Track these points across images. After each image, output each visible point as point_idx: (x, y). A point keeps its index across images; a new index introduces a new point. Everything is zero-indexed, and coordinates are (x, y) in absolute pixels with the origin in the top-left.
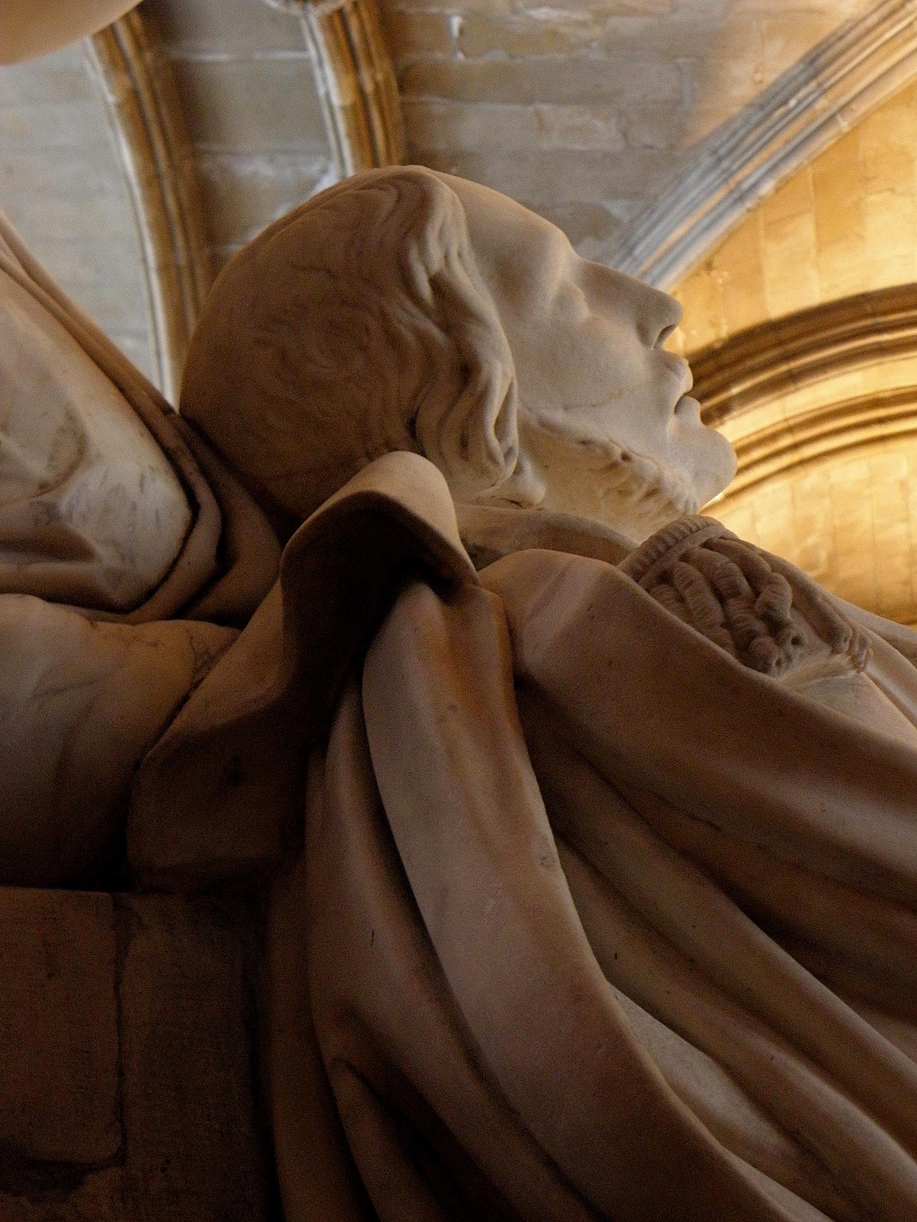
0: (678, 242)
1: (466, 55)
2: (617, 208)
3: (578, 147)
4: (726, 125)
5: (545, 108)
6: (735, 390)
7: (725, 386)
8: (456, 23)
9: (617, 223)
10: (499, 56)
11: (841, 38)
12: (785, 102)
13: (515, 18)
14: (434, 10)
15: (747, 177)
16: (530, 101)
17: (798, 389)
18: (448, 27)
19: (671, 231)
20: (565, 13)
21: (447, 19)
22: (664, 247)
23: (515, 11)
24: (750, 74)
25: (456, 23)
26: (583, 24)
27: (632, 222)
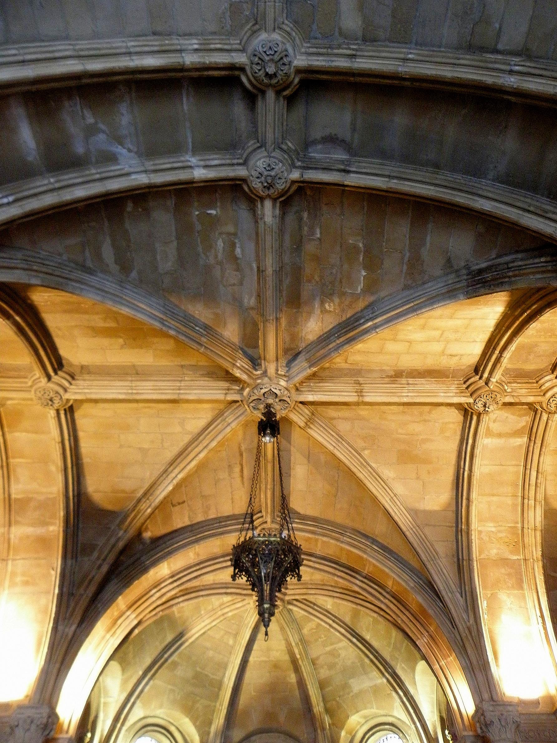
0: (138, 306)
1: (197, 215)
2: (134, 274)
3: (158, 257)
4: (176, 305)
5: (175, 243)
6: (18, 318)
7: (18, 314)
8: (213, 212)
9: (127, 276)
10: (198, 227)
11: (221, 337)
12: (196, 326)
13: (217, 234)
14: (218, 204)
15: (169, 322)
16: (178, 238)
17: (18, 336)
18: (211, 209)
19: (142, 303)
20: (221, 251)
21: (214, 208)
22: (136, 302)
23: (221, 234)
24: (200, 312)
25: (213, 212)
26: (216, 257)
27: (129, 281)
